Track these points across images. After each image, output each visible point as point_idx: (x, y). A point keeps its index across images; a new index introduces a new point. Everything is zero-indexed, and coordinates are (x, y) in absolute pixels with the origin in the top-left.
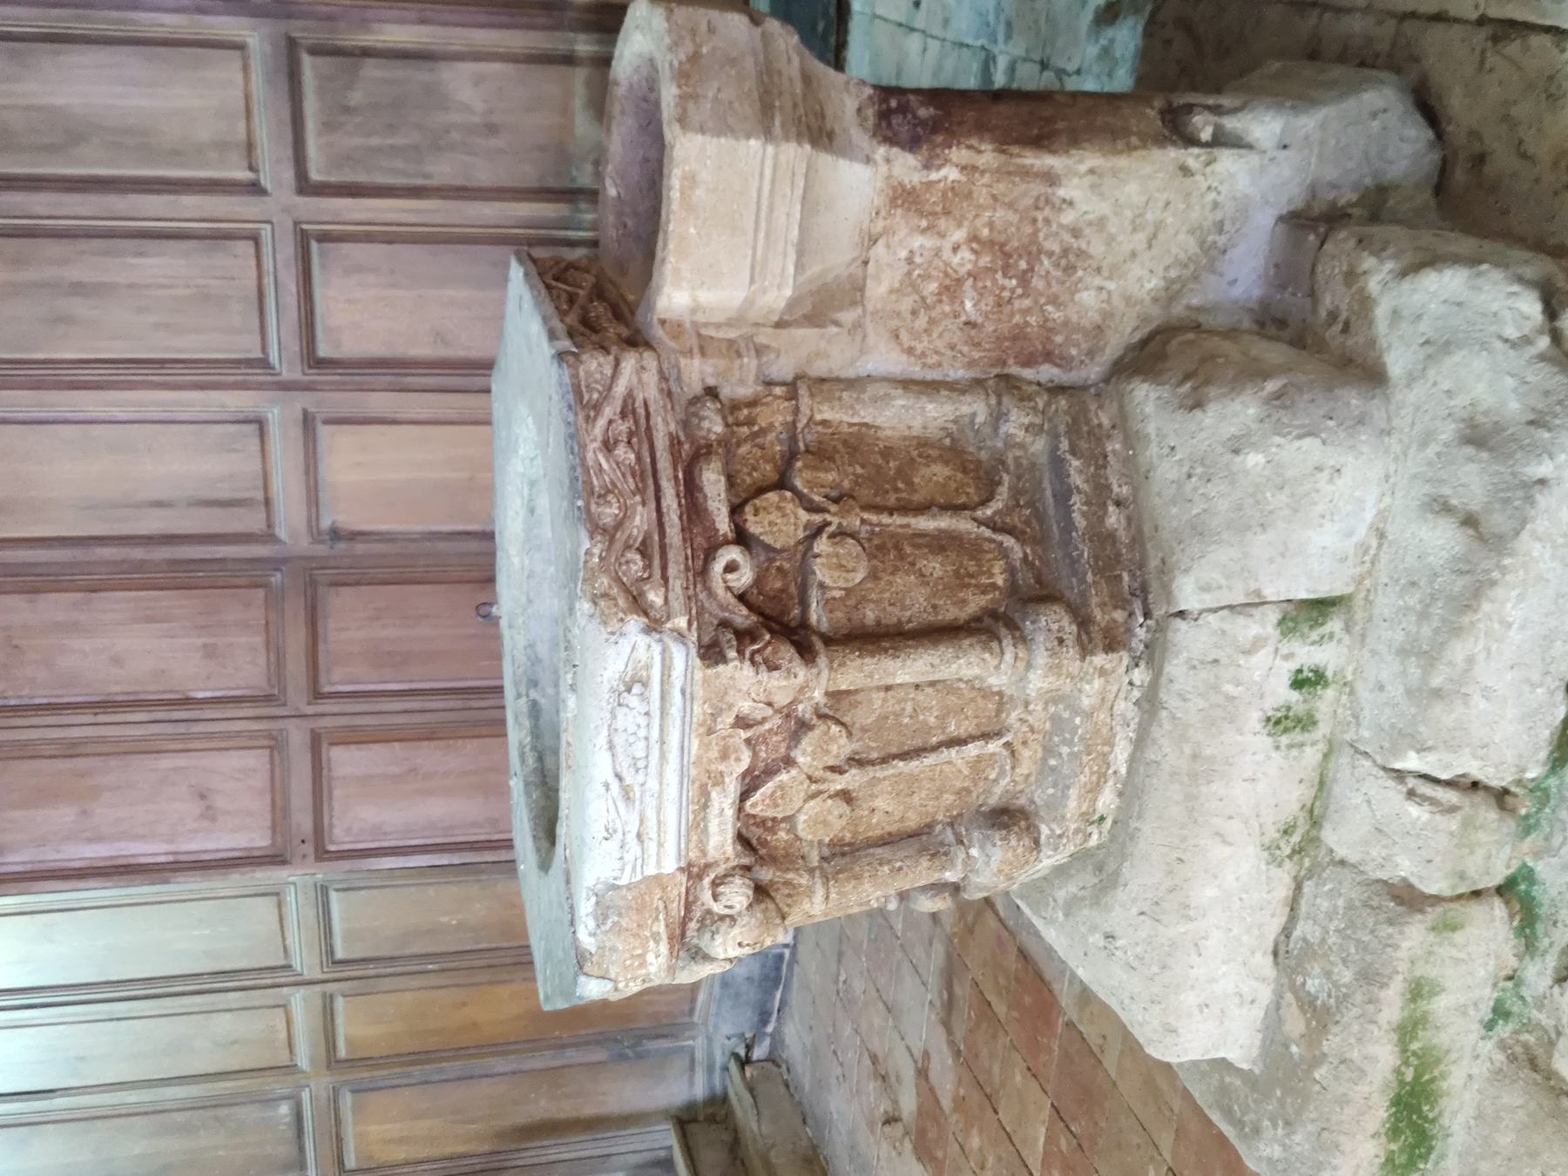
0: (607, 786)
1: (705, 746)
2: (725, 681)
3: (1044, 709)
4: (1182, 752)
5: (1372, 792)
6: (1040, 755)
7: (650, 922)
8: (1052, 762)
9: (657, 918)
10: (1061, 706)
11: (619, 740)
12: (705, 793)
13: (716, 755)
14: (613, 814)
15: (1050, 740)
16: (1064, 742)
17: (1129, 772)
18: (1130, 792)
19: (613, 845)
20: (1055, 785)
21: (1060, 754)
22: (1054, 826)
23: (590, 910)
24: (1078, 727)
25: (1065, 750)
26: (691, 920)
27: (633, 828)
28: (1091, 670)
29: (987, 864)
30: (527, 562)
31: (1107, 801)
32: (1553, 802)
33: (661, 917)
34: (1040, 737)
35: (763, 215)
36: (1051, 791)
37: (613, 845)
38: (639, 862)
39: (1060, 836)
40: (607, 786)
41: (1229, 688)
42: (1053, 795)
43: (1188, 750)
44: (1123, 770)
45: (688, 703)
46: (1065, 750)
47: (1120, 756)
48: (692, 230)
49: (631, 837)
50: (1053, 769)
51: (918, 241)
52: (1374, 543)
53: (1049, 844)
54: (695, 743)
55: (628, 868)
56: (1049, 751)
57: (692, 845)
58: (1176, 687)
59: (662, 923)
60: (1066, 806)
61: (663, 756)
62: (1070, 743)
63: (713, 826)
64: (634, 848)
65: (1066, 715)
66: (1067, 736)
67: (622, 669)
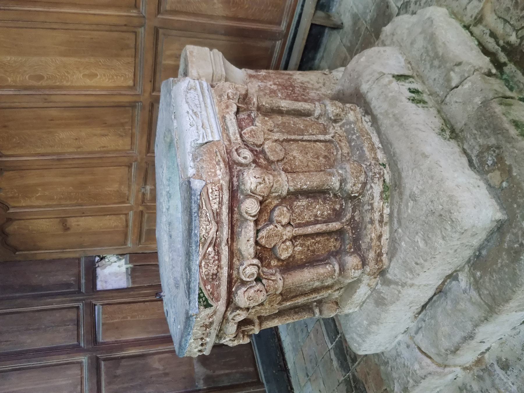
0: (188, 112)
1: (220, 106)
2: (221, 87)
3: (341, 129)
4: (390, 118)
5: (455, 99)
6: (348, 145)
7: (214, 158)
8: (353, 144)
9: (217, 155)
10: (345, 126)
11: (189, 100)
12: (224, 118)
13: (224, 107)
14: (192, 119)
15: (348, 138)
16: (353, 135)
17: (382, 146)
18: (386, 146)
19: (194, 128)
20: (358, 150)
21: (354, 139)
22: (366, 163)
23: (191, 159)
24: (354, 128)
25: (354, 137)
26: (234, 176)
27: (200, 124)
28: (347, 109)
29: (346, 172)
30: (171, 255)
31: (380, 155)
32: (510, 80)
33: (218, 153)
34: (345, 138)
35: (213, 62)
36: (358, 153)
37: (194, 128)
38: (205, 134)
39: (370, 165)
40: (188, 112)
41: (390, 94)
42: (359, 153)
43: (391, 116)
44: (380, 146)
45: (212, 99)
46: (354, 137)
47: (375, 139)
48: (194, 60)
49: (200, 127)
50: (354, 146)
51: (260, 84)
52: (409, 66)
53: (368, 170)
54: (217, 108)
55: (201, 137)
56: (350, 142)
57: (225, 138)
58: (377, 107)
59: (219, 156)
60: (366, 154)
61: (206, 106)
62: (355, 134)
63: (229, 124)
64: (202, 131)
65: (348, 127)
66: (352, 132)
67: (187, 86)
